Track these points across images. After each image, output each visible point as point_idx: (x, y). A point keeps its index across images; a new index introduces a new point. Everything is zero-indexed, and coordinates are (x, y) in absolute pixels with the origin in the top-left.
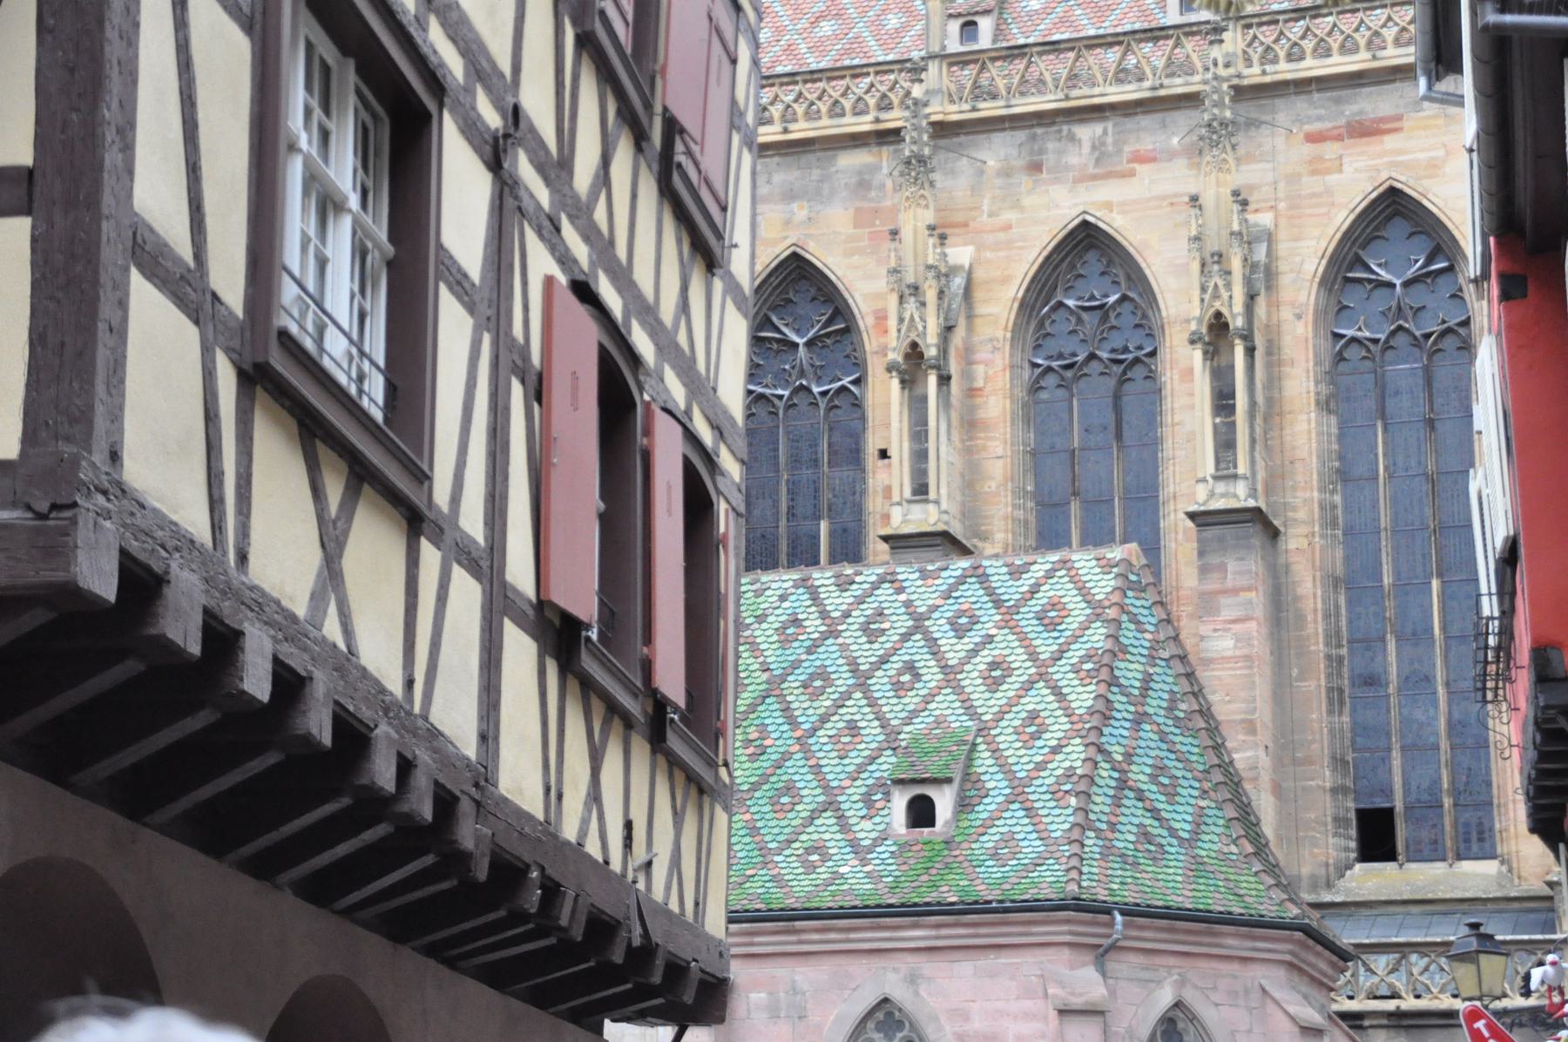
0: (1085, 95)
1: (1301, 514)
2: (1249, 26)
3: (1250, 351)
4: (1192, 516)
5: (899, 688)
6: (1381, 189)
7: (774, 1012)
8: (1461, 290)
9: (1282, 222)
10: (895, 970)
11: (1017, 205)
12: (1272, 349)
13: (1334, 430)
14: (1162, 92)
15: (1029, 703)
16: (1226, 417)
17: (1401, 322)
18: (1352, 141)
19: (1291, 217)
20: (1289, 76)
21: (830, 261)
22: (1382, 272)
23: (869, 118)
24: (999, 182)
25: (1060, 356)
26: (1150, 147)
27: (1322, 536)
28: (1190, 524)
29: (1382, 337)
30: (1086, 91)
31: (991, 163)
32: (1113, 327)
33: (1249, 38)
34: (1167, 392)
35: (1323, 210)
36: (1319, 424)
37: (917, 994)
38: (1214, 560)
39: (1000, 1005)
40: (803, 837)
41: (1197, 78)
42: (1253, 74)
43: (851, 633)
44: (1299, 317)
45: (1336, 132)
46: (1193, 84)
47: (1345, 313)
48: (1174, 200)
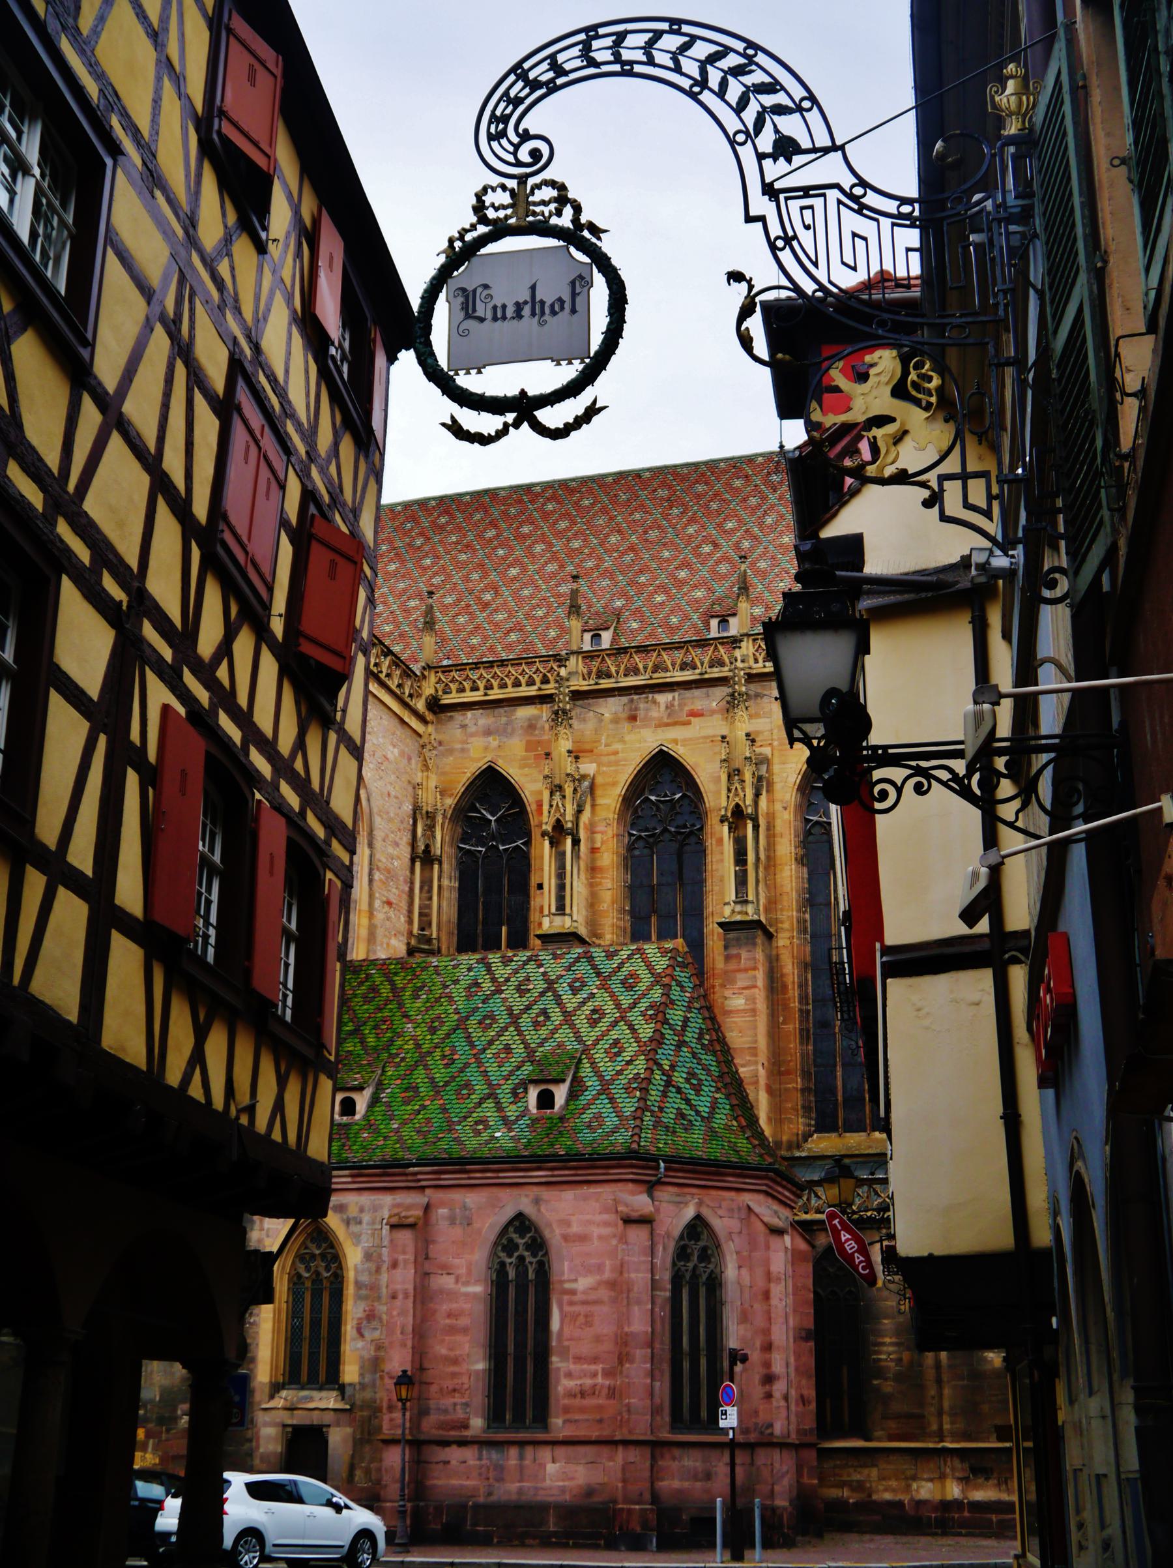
0: (660, 677)
1: (786, 925)
2: (754, 640)
3: (756, 827)
4: (721, 924)
5: (536, 1025)
7: (452, 1221)
9: (776, 753)
10: (527, 1196)
11: (622, 740)
12: (770, 827)
13: (806, 876)
14: (706, 676)
15: (614, 1034)
21: (511, 772)
23: (535, 687)
24: (611, 726)
25: (647, 830)
27: (798, 938)
28: (721, 930)
30: (662, 674)
31: (607, 715)
32: (677, 813)
34: (708, 852)
37: (539, 1210)
38: (734, 951)
39: (589, 1217)
40: (475, 1115)
41: (726, 669)
43: (509, 992)
44: (785, 809)
46: (724, 672)
47: (813, 807)
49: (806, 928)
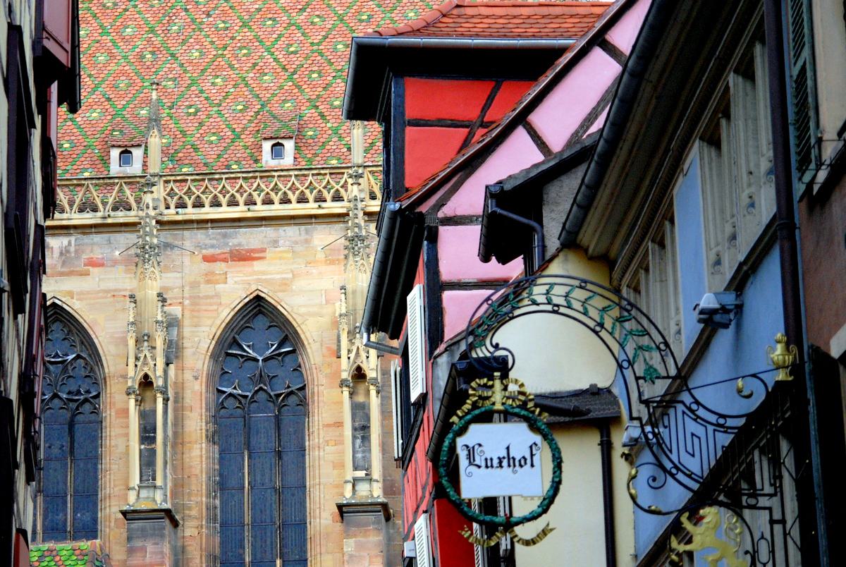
1: (194, 513)
2: (167, 182)
3: (166, 400)
4: (124, 513)
6: (251, 297)
8: (300, 366)
9: (187, 314)
12: (178, 398)
13: (217, 456)
14: (109, 221)
16: (148, 444)
17: (262, 385)
18: (233, 262)
19: (193, 311)
20: (194, 217)
22: (251, 351)
26: (100, 256)
27: (207, 528)
28: (121, 516)
29: (250, 394)
32: (70, 377)
33: (168, 190)
34: (106, 423)
35: (215, 307)
36: (207, 451)
38: (138, 543)
41: (132, 213)
42: (171, 214)
44: (196, 378)
45: (223, 256)
46: (131, 217)
47: (226, 376)
48: (115, 294)
49: (215, 515)
